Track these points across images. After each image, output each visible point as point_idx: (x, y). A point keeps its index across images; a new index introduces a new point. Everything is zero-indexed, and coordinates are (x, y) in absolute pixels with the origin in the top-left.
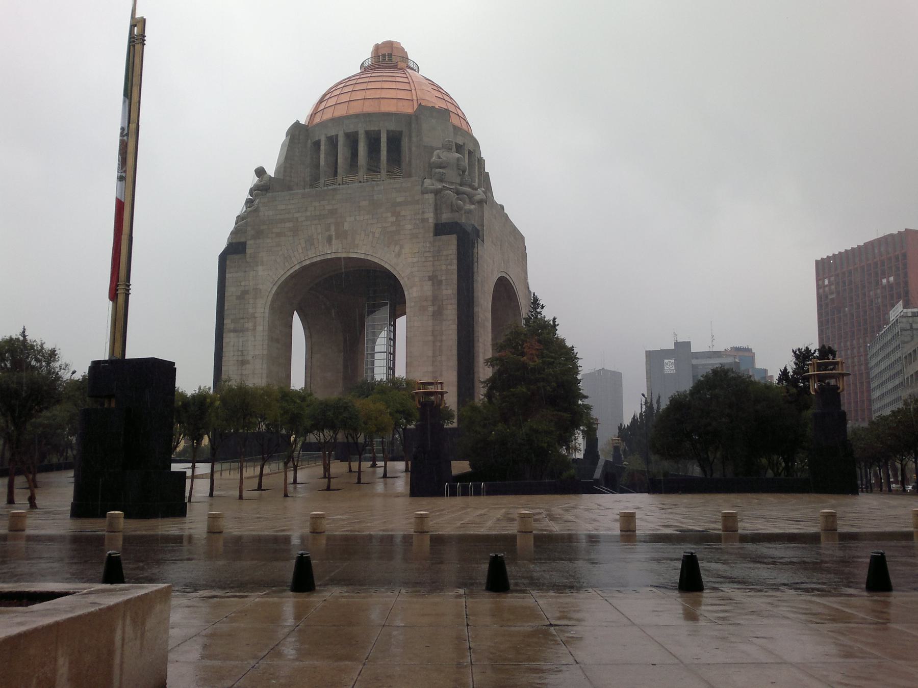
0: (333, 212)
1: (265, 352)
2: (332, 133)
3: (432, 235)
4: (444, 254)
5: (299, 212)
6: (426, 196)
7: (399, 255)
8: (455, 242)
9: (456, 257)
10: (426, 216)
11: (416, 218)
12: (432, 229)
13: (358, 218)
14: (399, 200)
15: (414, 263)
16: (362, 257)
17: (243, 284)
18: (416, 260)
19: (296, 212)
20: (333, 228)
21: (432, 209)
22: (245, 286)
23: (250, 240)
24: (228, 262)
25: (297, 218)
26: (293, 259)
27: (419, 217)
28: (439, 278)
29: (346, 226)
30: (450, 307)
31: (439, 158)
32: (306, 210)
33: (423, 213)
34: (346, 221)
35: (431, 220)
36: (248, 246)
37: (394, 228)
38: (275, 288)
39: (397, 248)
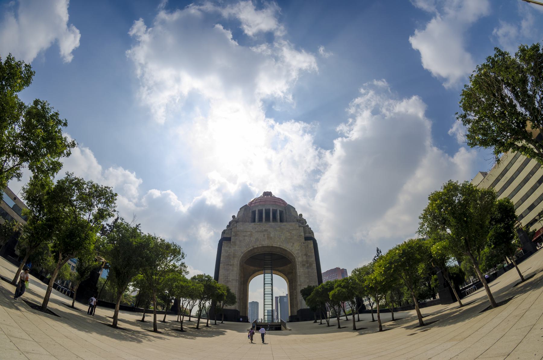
0: (266, 230)
1: (237, 278)
2: (261, 208)
6: (301, 228)
7: (292, 246)
8: (312, 243)
9: (313, 248)
10: (301, 234)
12: (304, 238)
14: (291, 228)
17: (229, 252)
18: (299, 248)
20: (266, 235)
21: (303, 232)
22: (230, 253)
23: (233, 237)
24: (223, 243)
25: (252, 231)
26: (250, 245)
27: (298, 234)
28: (308, 254)
29: (271, 236)
30: (314, 264)
31: (300, 218)
32: (256, 229)
33: (300, 233)
35: (303, 235)
36: (232, 239)
37: (290, 238)
38: (242, 255)
39: (292, 244)
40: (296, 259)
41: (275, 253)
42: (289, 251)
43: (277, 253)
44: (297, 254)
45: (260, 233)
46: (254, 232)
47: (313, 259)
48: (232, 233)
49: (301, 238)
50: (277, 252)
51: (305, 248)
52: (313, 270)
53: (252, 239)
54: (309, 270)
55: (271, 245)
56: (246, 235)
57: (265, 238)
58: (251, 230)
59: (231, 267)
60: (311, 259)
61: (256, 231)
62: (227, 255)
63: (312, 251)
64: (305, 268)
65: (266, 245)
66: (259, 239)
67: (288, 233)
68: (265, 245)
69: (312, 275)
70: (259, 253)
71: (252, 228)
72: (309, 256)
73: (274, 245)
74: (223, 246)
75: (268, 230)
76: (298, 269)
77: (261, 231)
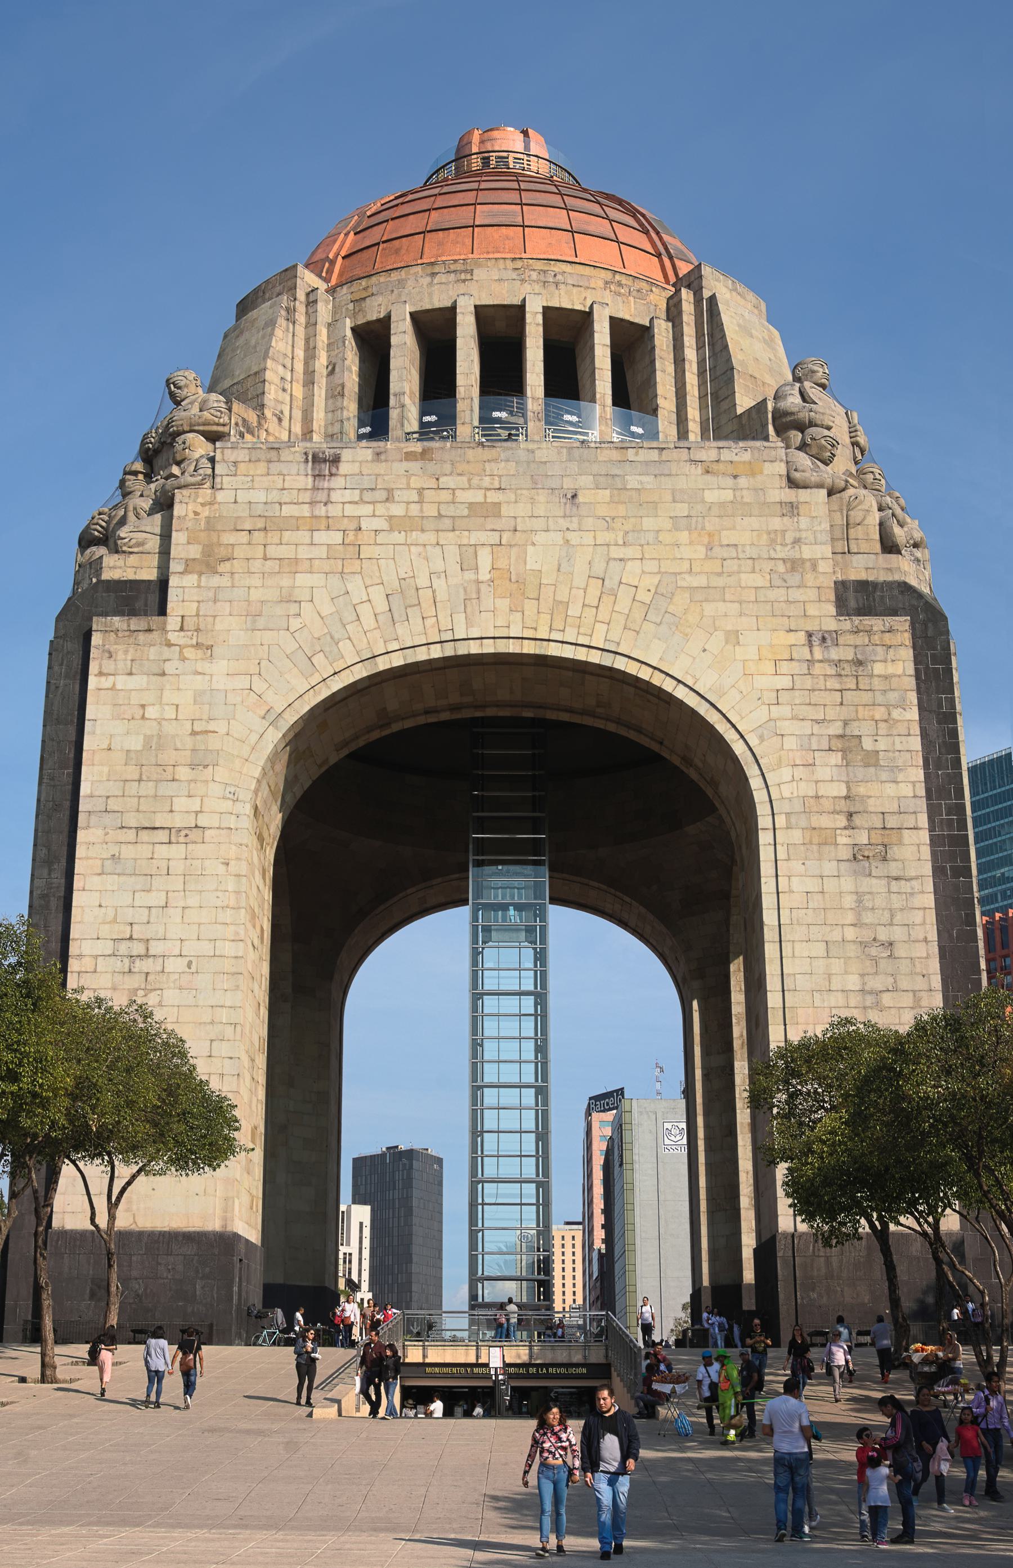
3: (832, 610)
4: (876, 672)
5: (362, 501)
6: (803, 495)
8: (907, 638)
9: (911, 683)
10: (807, 552)
11: (773, 555)
13: (574, 538)
14: (710, 496)
15: (778, 691)
16: (595, 658)
18: (785, 682)
19: (350, 502)
22: (159, 721)
24: (96, 639)
26: (345, 647)
27: (782, 552)
33: (797, 541)
34: (533, 544)
37: (701, 581)
40: (755, 783)
41: (565, 717)
42: (691, 701)
43: (588, 721)
44: (762, 739)
45: (430, 537)
46: (381, 524)
47: (907, 790)
48: (178, 538)
49: (801, 586)
50: (583, 713)
51: (833, 683)
52: (905, 886)
53: (355, 586)
54: (868, 884)
55: (529, 648)
56: (304, 553)
57: (478, 582)
58: (350, 510)
59: (177, 851)
60: (890, 789)
61: (390, 518)
62: (135, 743)
63: (896, 714)
64: (829, 868)
65: (489, 648)
66: (426, 595)
67: (684, 536)
68: (474, 648)
69: (898, 934)
70: (422, 720)
71: (356, 495)
72: (872, 759)
73: (554, 650)
74: (93, 667)
75: (505, 510)
76: (766, 869)
77: (440, 516)
